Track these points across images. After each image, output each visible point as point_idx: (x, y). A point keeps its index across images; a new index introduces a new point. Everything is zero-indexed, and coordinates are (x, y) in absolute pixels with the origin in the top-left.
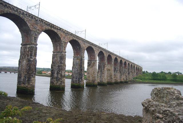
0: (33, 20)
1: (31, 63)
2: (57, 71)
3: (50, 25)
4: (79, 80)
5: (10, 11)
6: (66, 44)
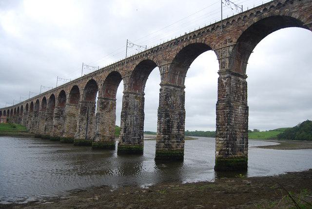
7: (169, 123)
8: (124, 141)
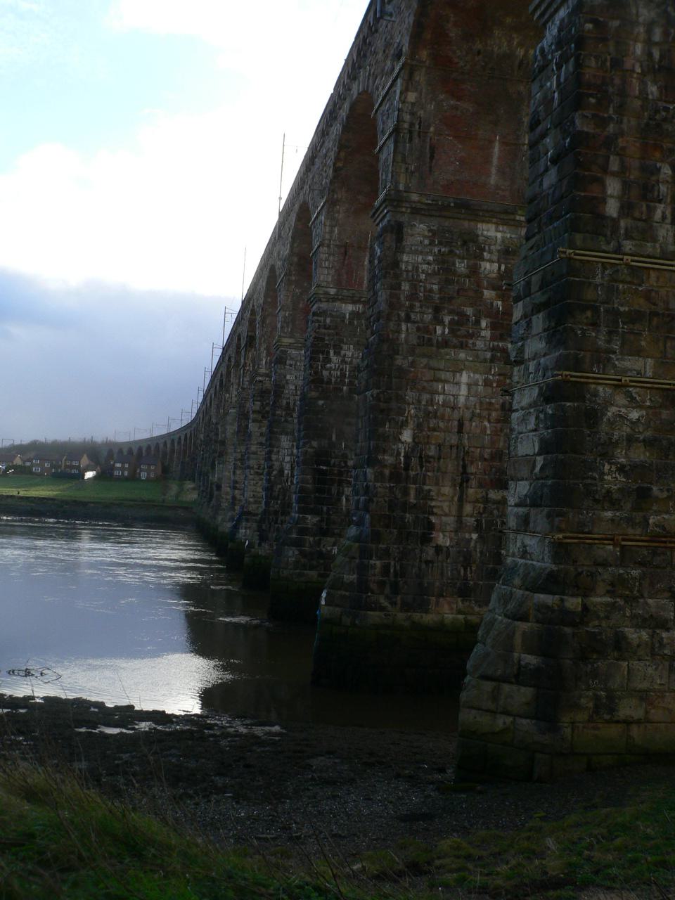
8: (263, 538)
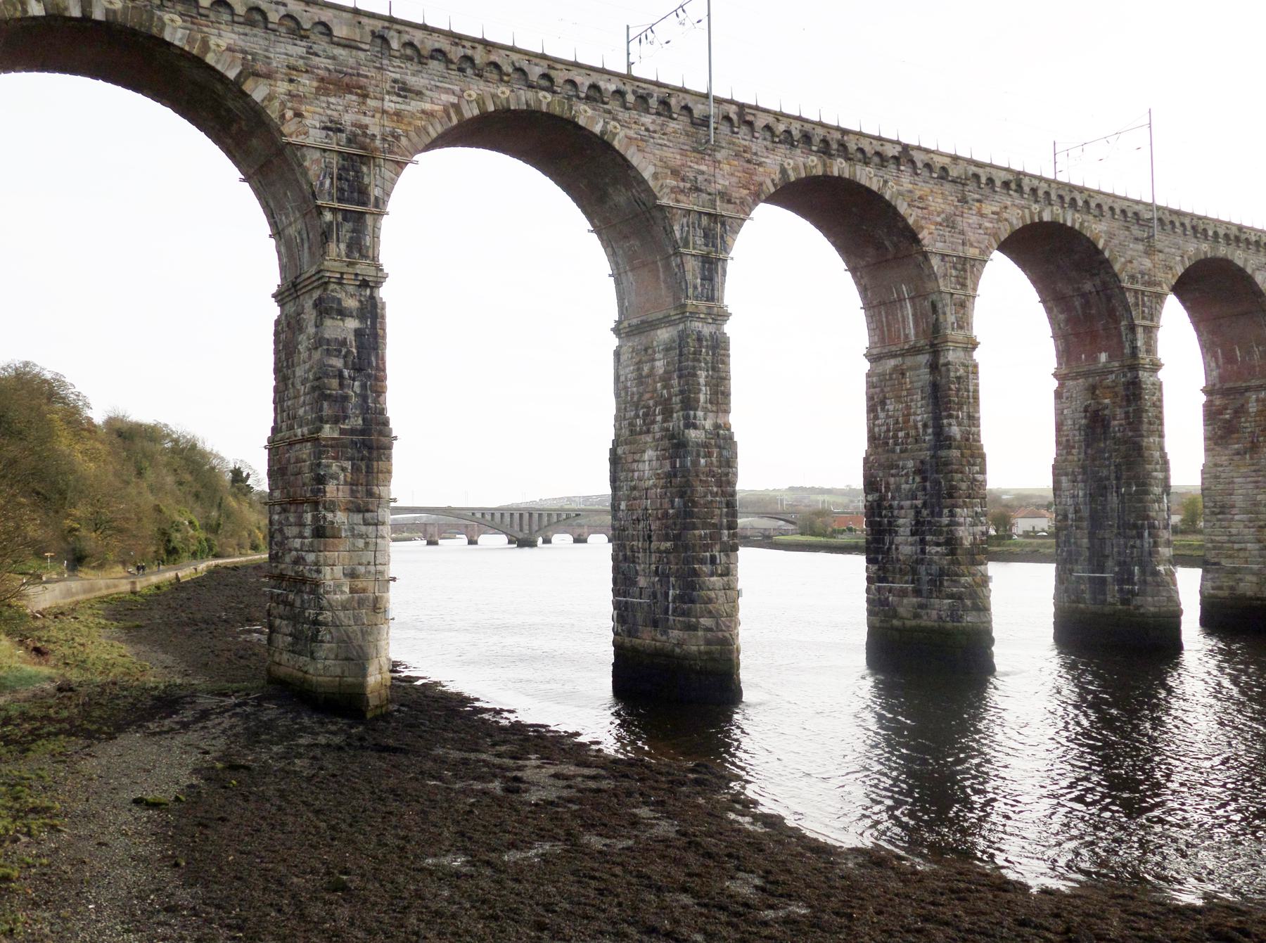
0: (673, 125)
1: (695, 463)
2: (918, 513)
3: (816, 140)
4: (1125, 577)
5: (503, 92)
6: (967, 269)
7: (880, 516)
